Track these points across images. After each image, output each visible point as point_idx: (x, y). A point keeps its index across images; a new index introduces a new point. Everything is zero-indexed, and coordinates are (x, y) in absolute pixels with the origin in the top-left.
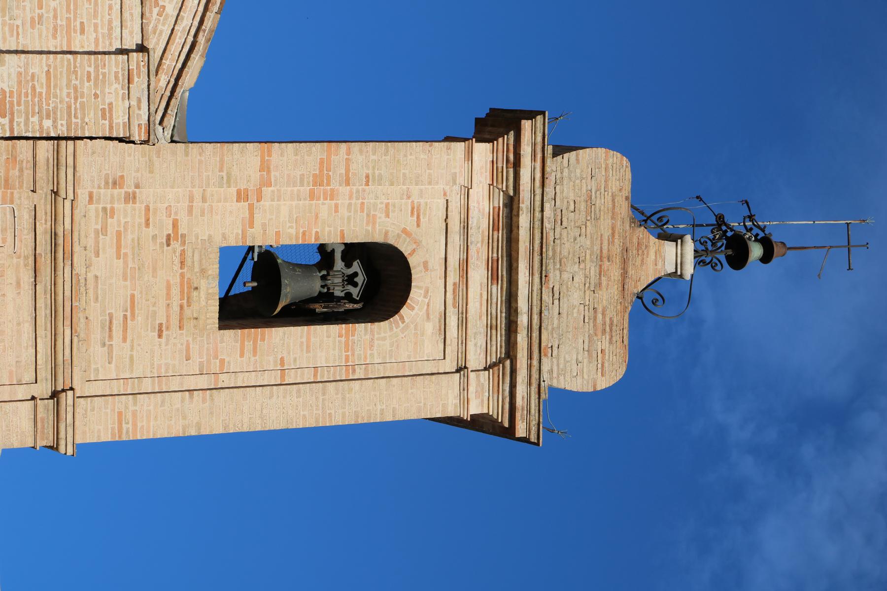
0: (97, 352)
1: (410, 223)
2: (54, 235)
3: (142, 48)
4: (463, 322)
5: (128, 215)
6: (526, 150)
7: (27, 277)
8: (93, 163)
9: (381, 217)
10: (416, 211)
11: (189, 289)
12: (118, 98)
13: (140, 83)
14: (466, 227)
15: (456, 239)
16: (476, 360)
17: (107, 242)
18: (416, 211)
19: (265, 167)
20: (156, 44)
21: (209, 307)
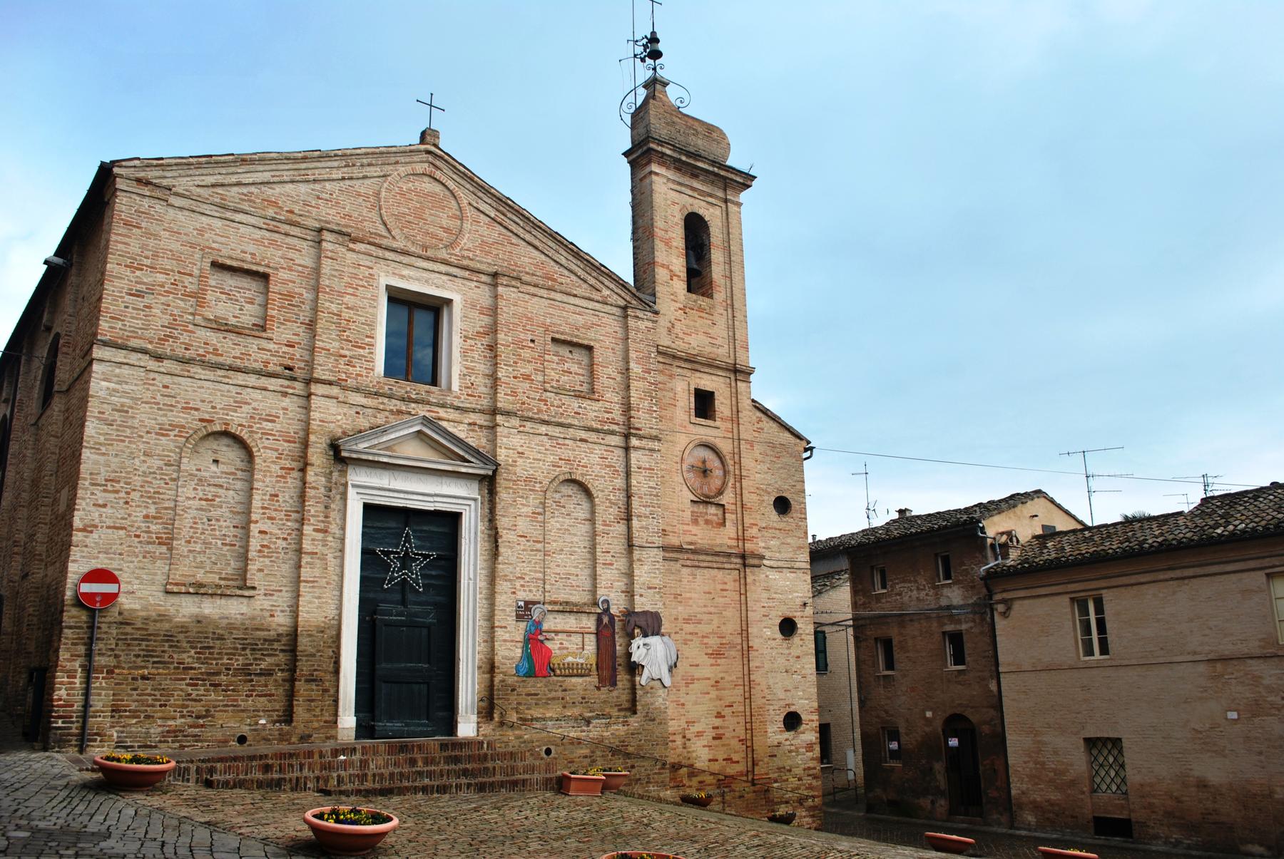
0: (720, 351)
1: (677, 207)
2: (686, 360)
3: (625, 308)
4: (711, 195)
5: (678, 328)
6: (659, 148)
7: (698, 374)
8: (665, 341)
9: (675, 220)
10: (674, 203)
11: (701, 309)
12: (640, 324)
13: (640, 314)
14: (680, 184)
15: (683, 189)
16: (720, 194)
17: (687, 339)
18: (674, 203)
19: (663, 266)
20: (622, 303)
21: (703, 302)
